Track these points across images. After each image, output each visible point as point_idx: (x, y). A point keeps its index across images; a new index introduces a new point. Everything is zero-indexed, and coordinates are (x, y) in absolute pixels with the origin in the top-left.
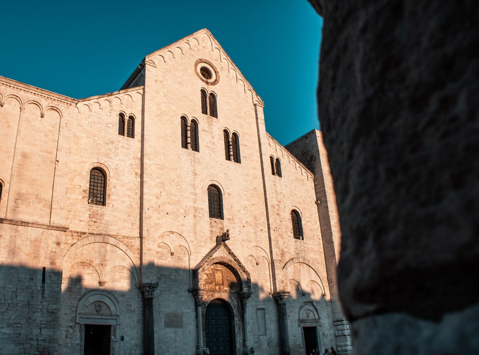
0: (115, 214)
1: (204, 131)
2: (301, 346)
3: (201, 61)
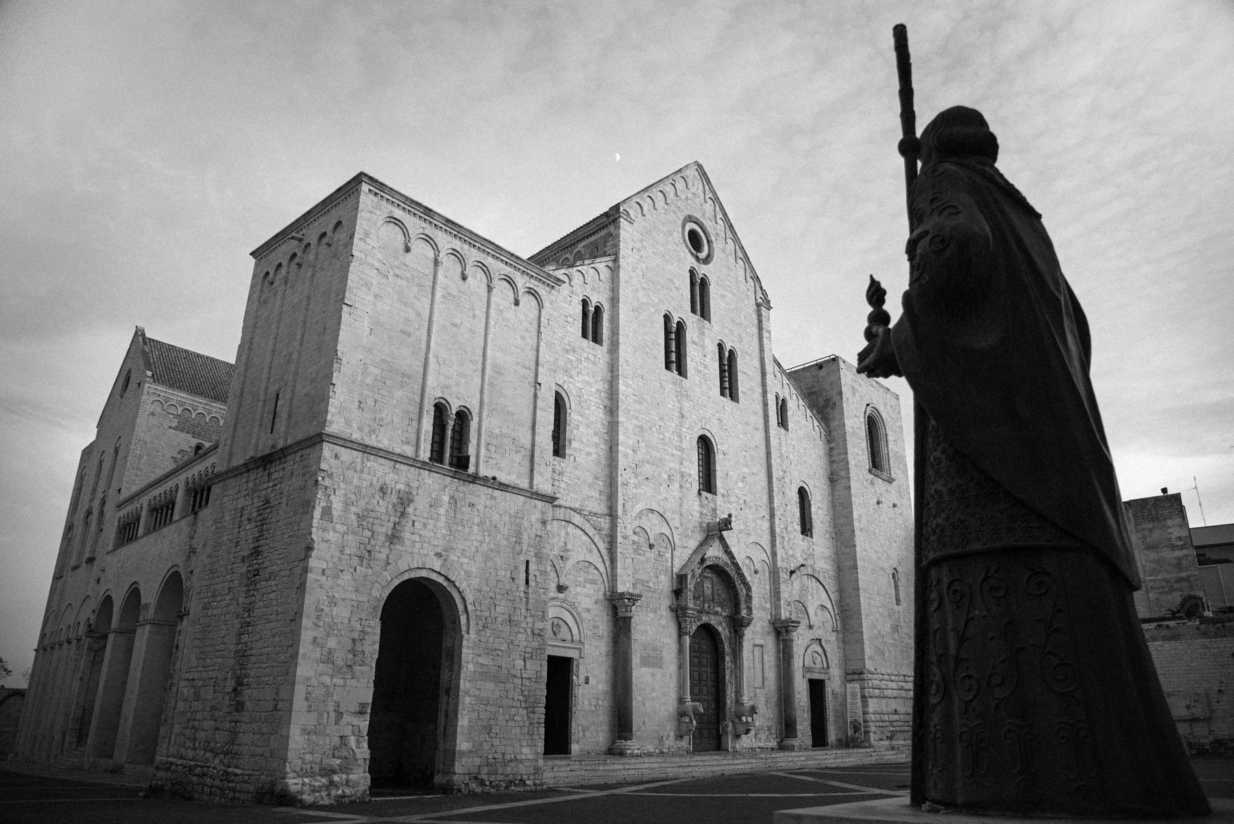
0: (577, 473)
1: (694, 342)
2: (806, 709)
3: (690, 219)
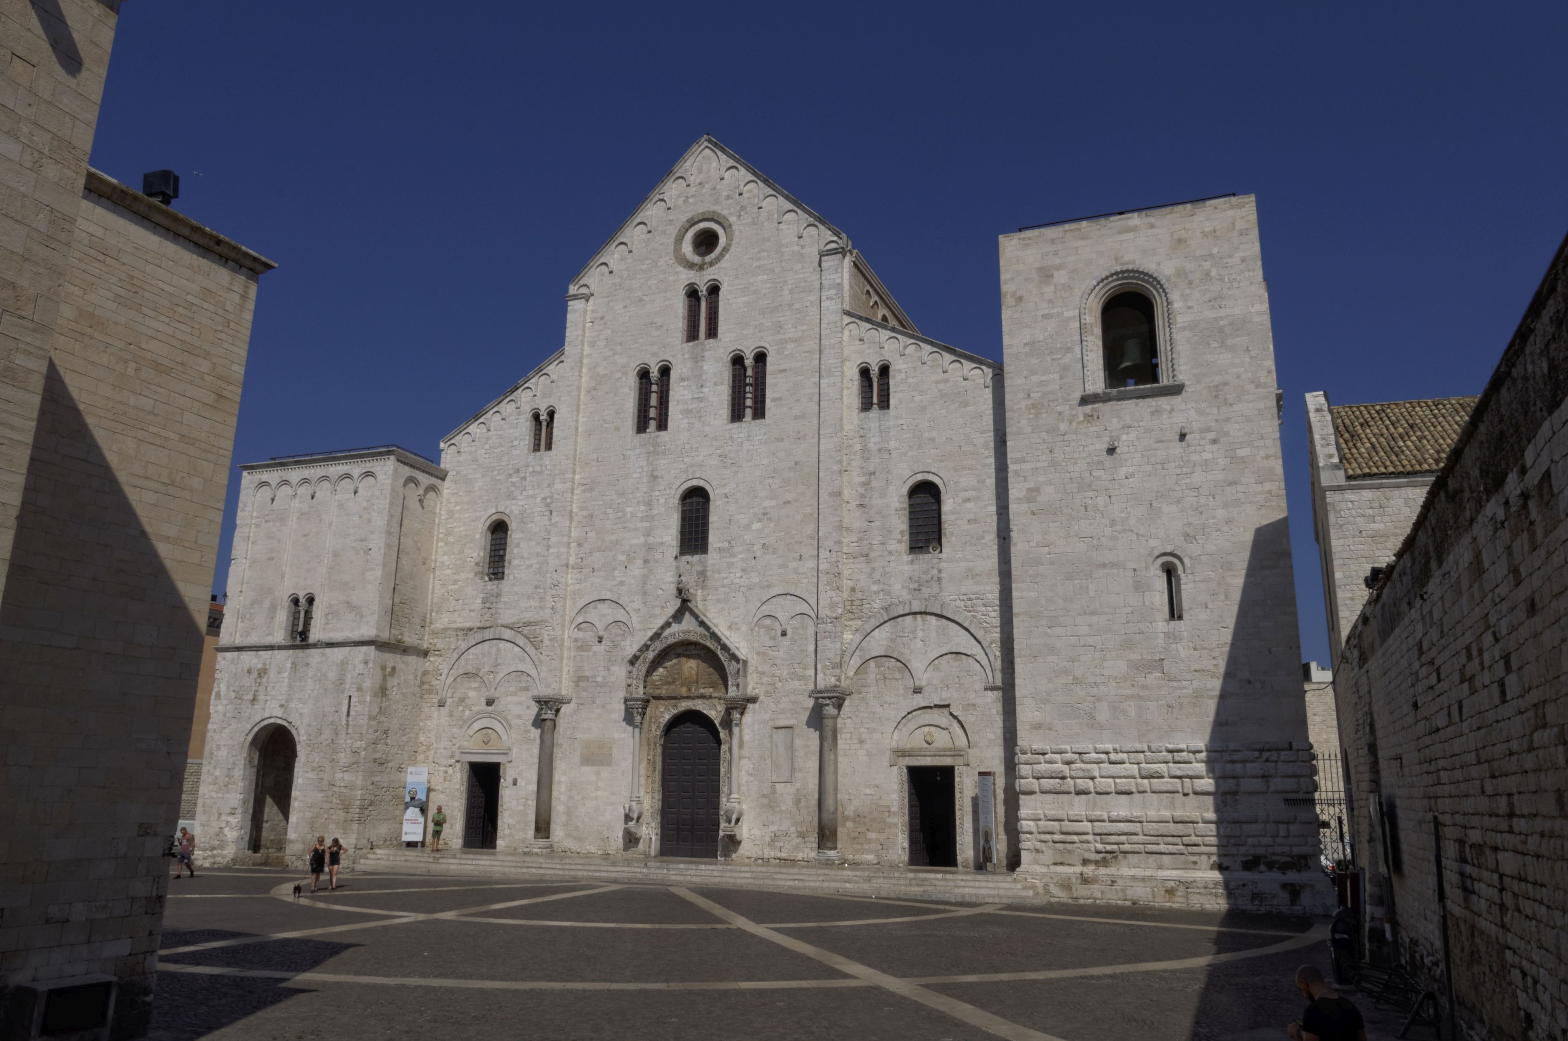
0: (516, 589)
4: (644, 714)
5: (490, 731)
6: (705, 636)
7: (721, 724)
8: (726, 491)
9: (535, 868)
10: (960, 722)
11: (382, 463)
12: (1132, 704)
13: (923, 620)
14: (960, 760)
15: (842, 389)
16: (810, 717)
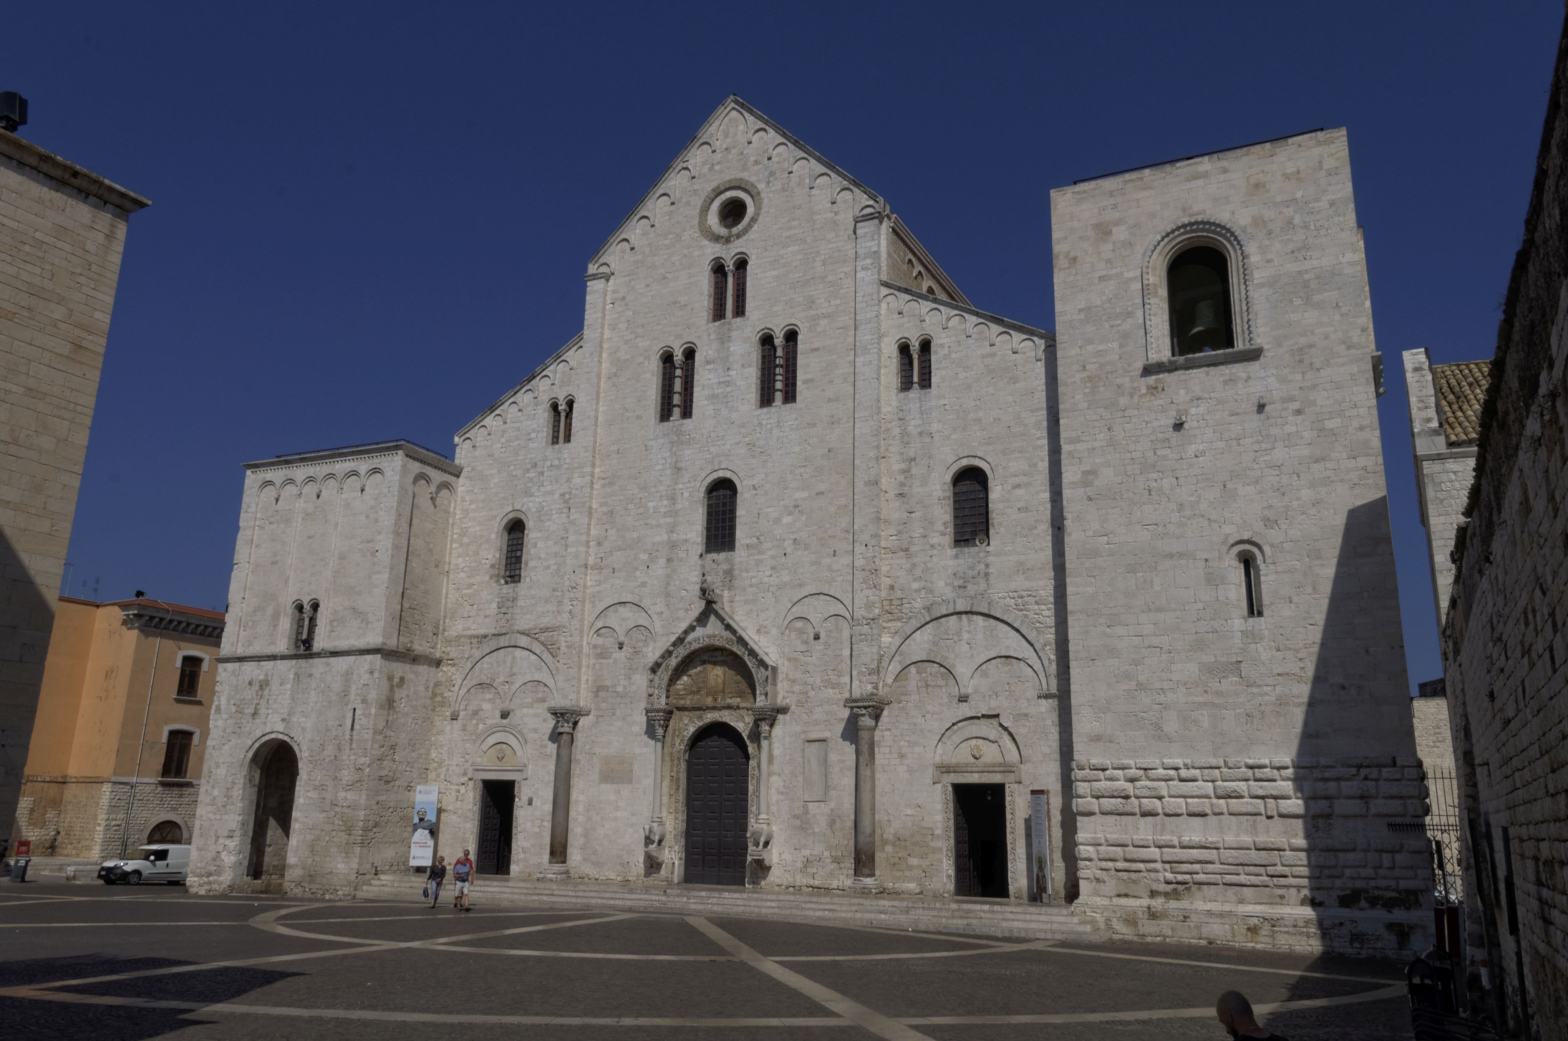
0: (533, 592)
4: (667, 727)
5: (504, 746)
6: (732, 641)
7: (749, 737)
8: (754, 482)
9: (547, 895)
10: (1011, 734)
11: (389, 458)
12: (1205, 712)
13: (969, 621)
14: (1011, 777)
15: (879, 368)
16: (845, 729)
